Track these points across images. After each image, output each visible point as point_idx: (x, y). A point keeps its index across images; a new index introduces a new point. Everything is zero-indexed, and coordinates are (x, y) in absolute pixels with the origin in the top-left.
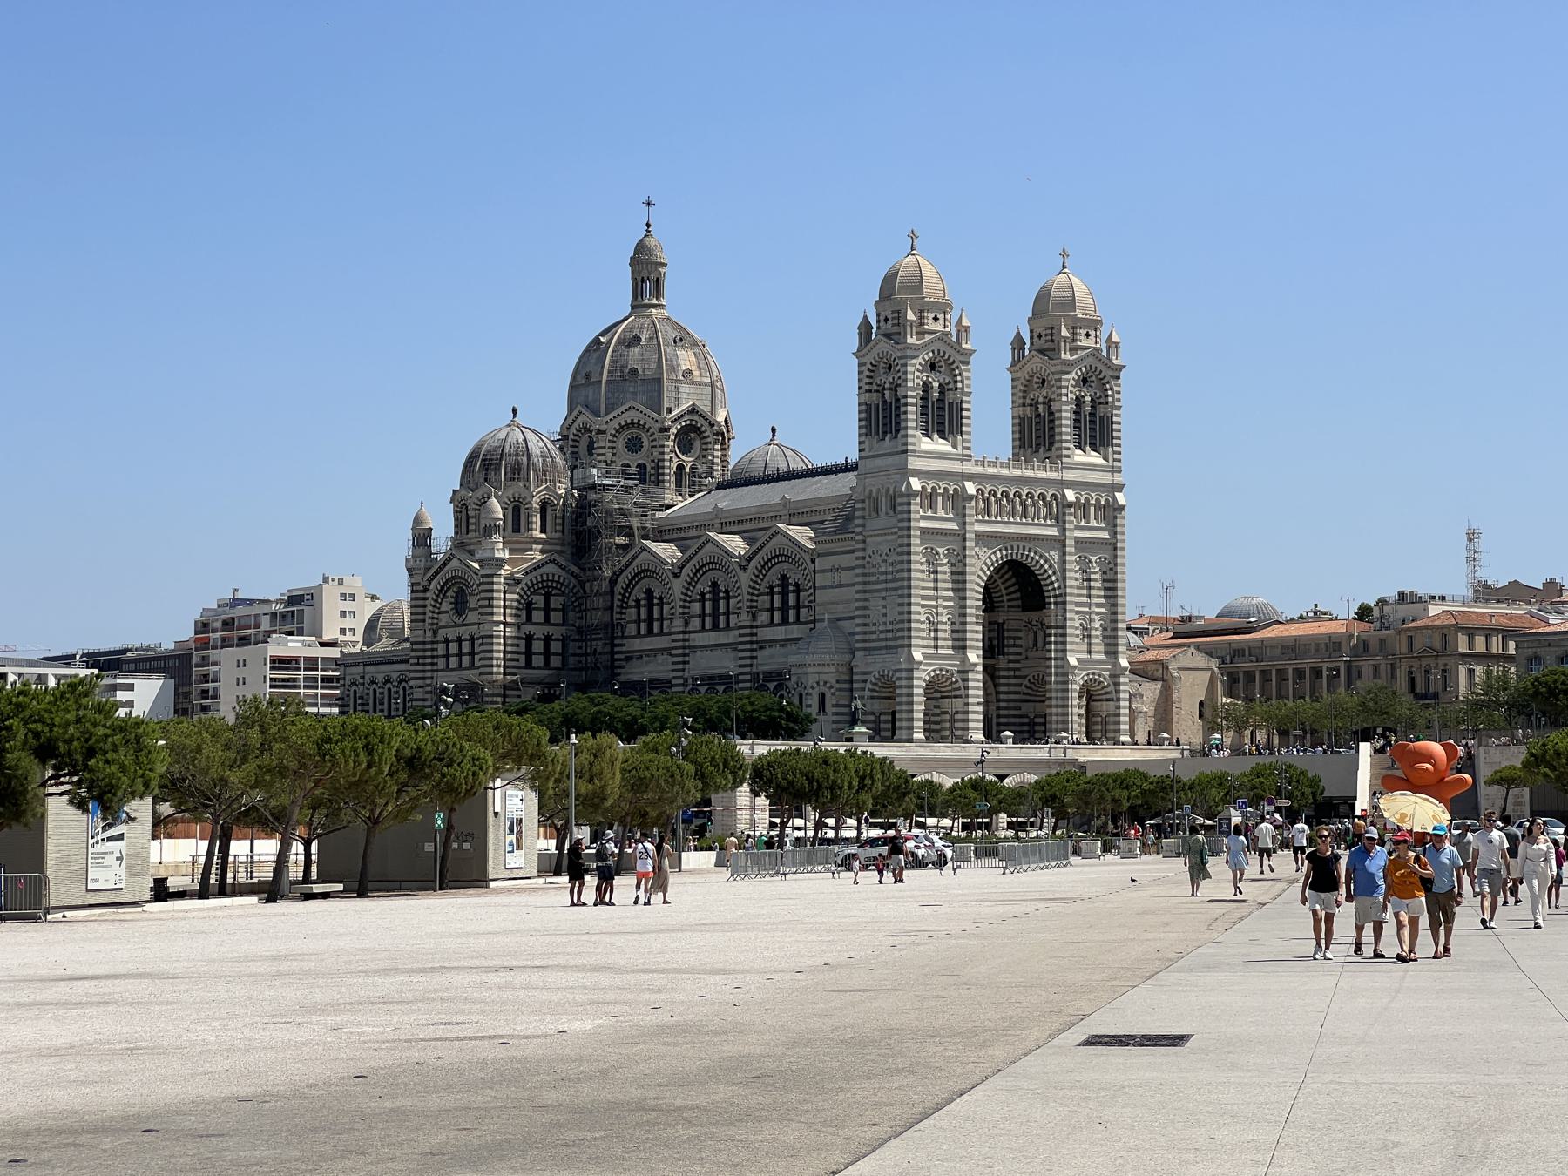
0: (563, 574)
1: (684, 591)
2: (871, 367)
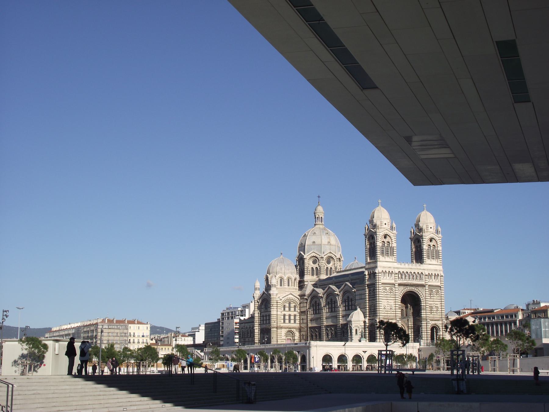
0: (293, 297)
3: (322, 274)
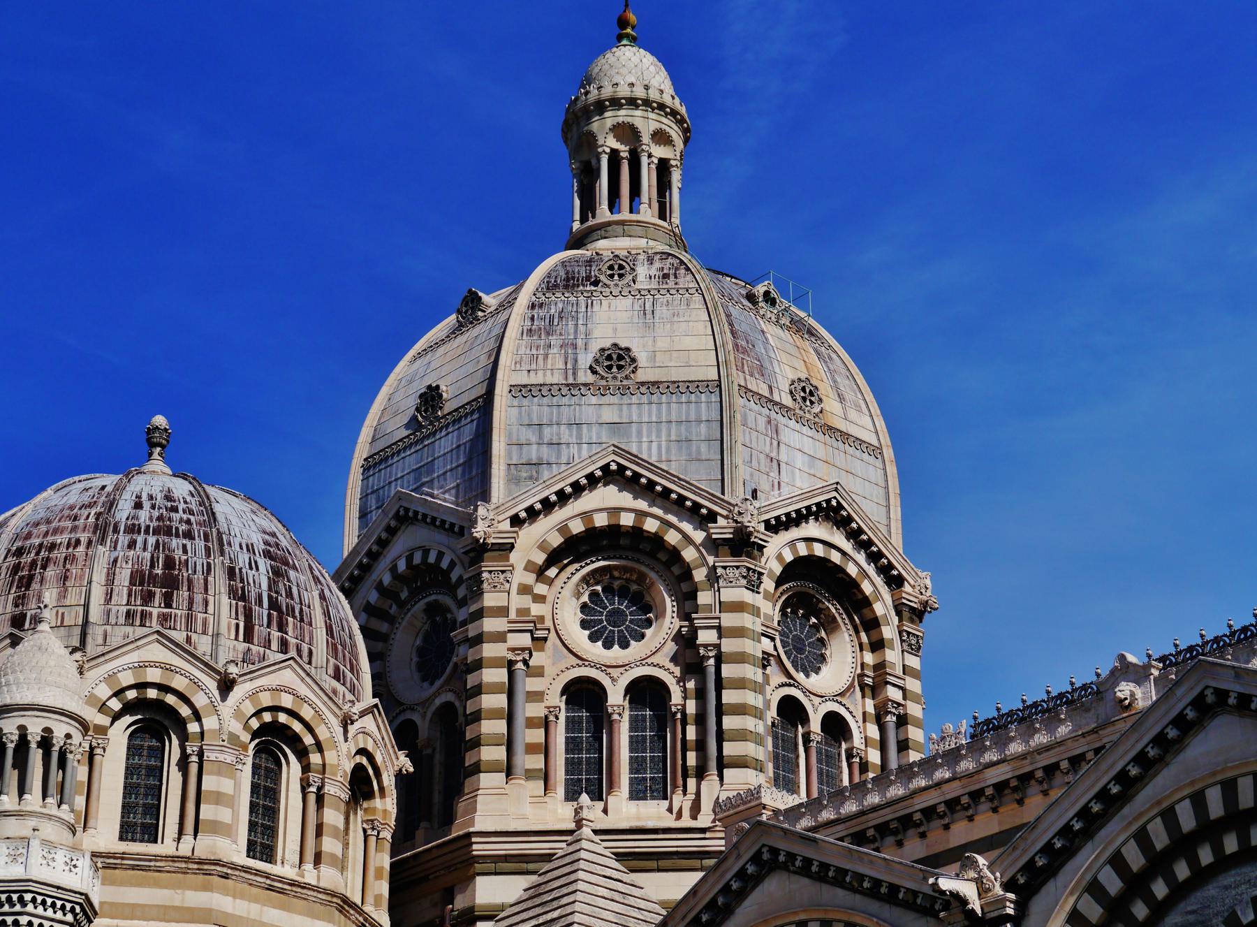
3: (741, 763)
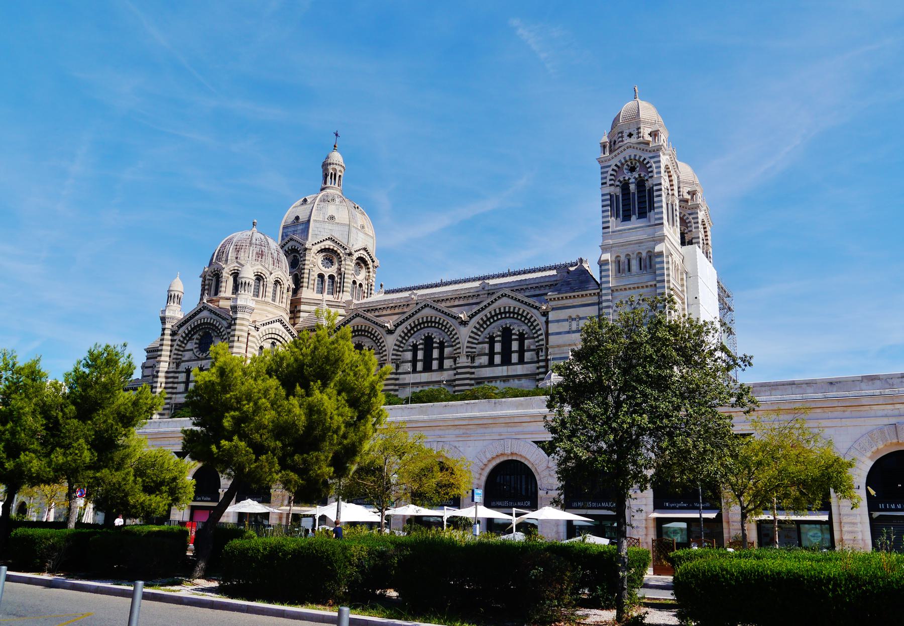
1: (398, 343)
2: (615, 168)
3: (346, 291)
